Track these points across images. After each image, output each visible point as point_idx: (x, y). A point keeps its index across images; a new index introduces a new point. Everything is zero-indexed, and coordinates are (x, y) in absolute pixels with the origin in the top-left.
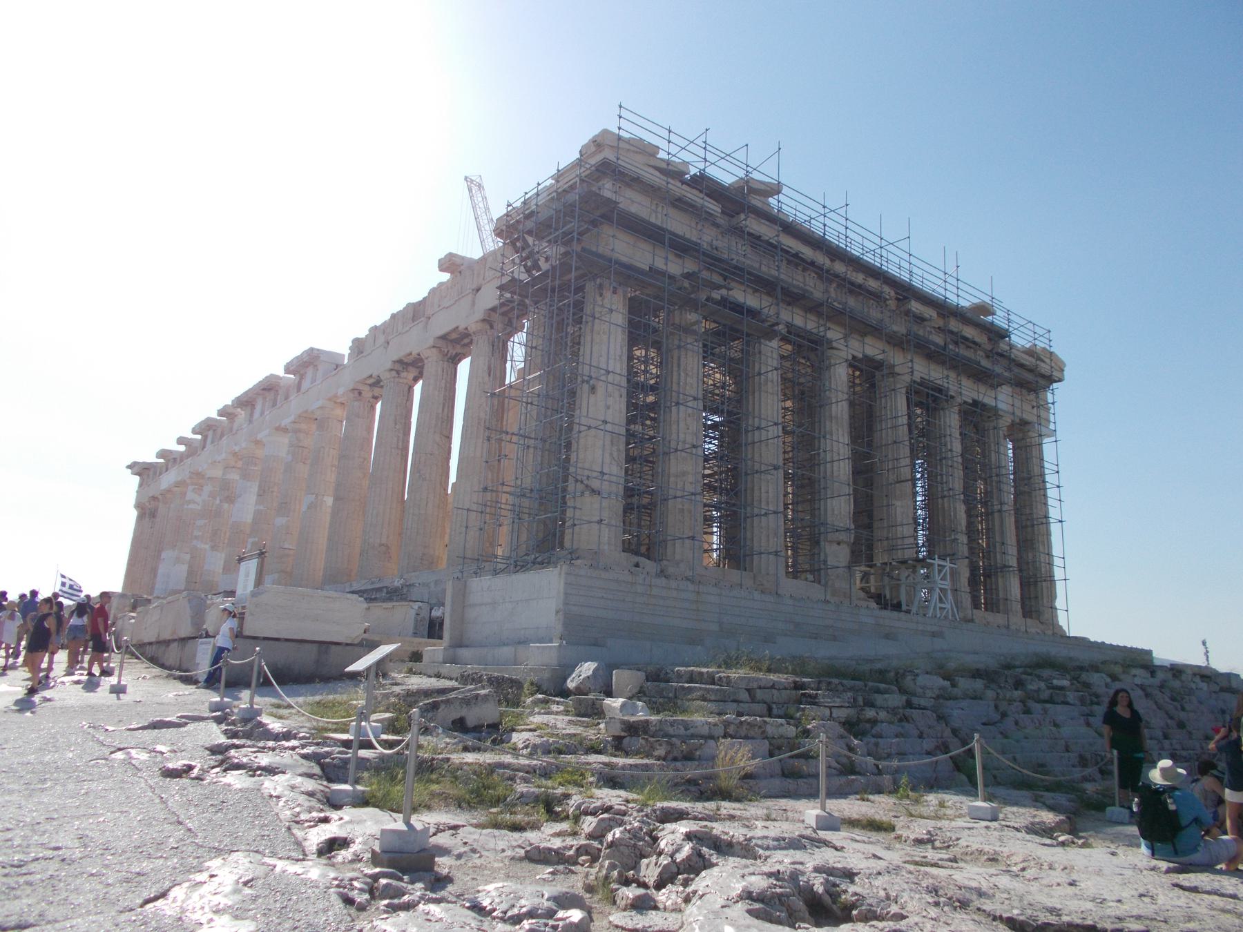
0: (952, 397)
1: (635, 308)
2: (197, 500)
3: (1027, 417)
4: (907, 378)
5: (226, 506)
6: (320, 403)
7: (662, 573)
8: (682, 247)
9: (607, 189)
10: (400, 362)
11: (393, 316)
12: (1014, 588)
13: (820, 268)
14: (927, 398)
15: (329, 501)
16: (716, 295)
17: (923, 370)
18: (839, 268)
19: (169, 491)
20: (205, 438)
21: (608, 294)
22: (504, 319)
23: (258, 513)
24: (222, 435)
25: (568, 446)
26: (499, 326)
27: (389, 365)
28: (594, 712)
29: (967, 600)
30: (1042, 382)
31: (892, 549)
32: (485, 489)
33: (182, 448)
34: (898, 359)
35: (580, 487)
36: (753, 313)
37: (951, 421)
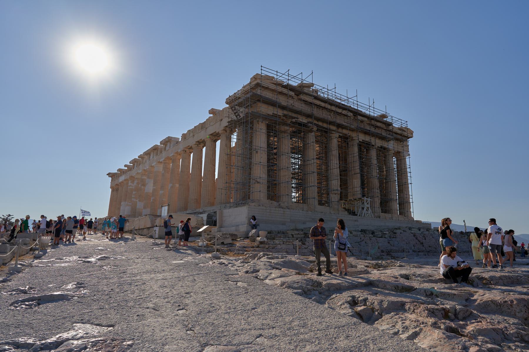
0: (373, 146)
1: (268, 127)
2: (132, 185)
3: (400, 151)
4: (358, 141)
5: (143, 187)
6: (172, 154)
7: (280, 206)
8: (283, 108)
9: (259, 91)
10: (198, 142)
11: (195, 127)
12: (396, 206)
13: (327, 109)
14: (364, 147)
15: (177, 185)
16: (294, 120)
17: (362, 137)
18: (333, 108)
19: (122, 182)
20: (134, 165)
21: (260, 123)
22: (230, 129)
23: (154, 190)
24: (140, 164)
25: (250, 169)
26: (228, 131)
27: (195, 143)
28: (254, 240)
29: (378, 210)
30: (404, 138)
31: (354, 195)
32: (226, 183)
33: (126, 168)
34: (354, 135)
35: (254, 181)
36: (305, 125)
37: (373, 153)
